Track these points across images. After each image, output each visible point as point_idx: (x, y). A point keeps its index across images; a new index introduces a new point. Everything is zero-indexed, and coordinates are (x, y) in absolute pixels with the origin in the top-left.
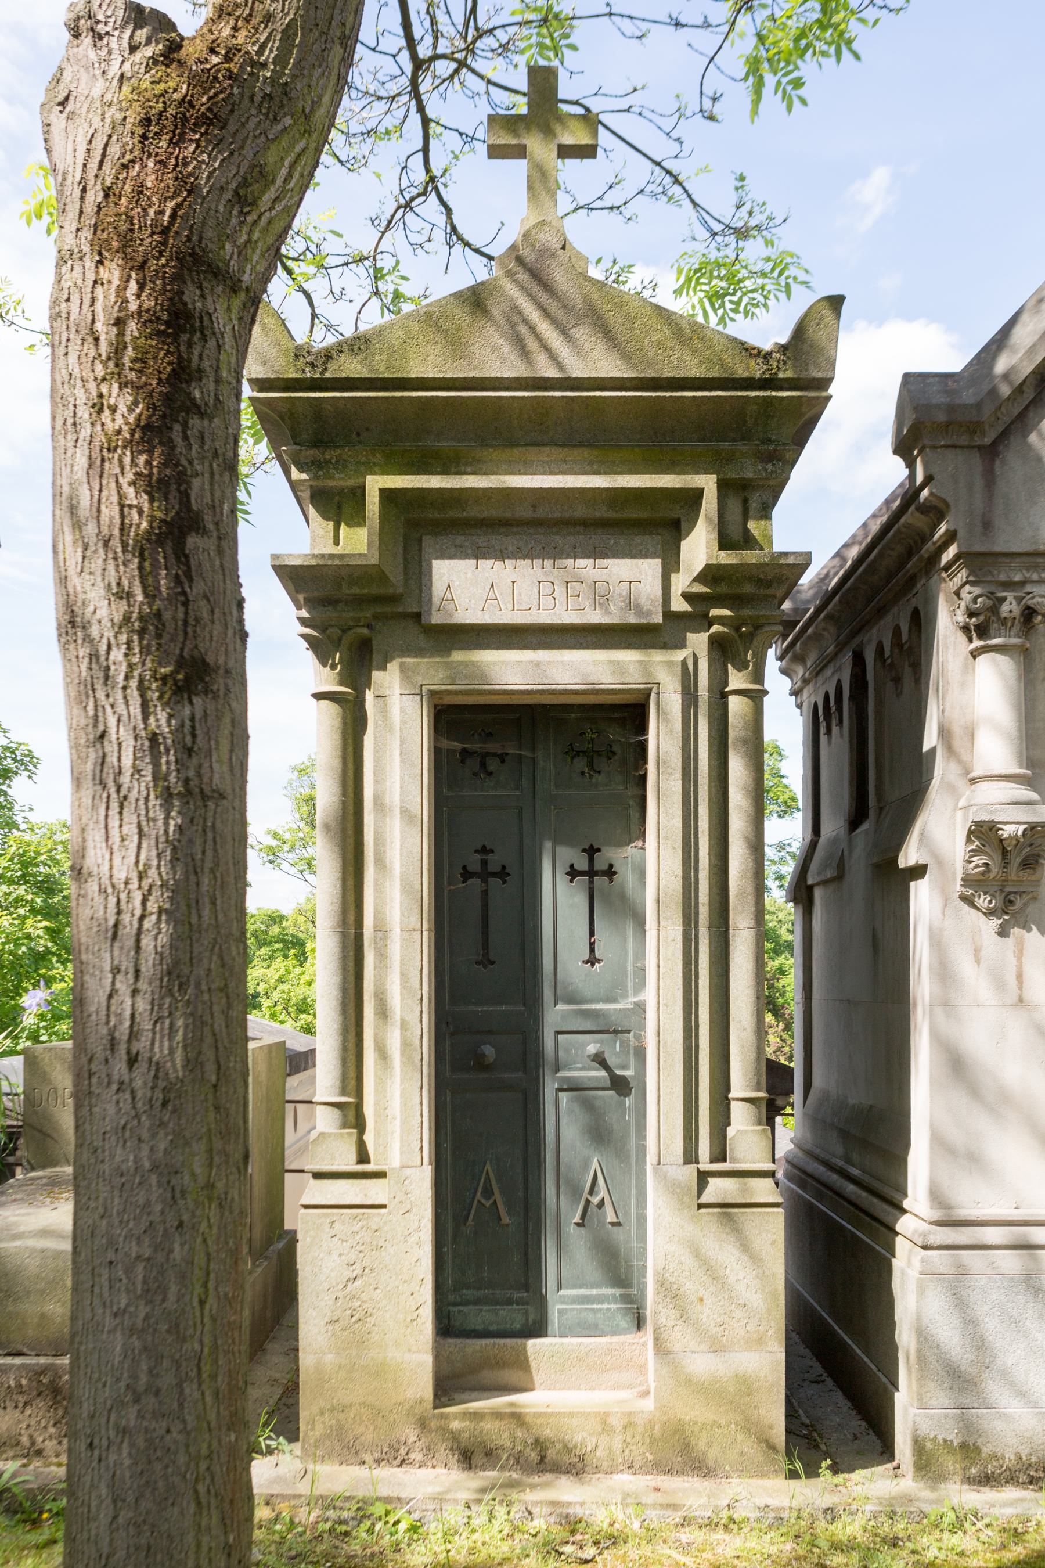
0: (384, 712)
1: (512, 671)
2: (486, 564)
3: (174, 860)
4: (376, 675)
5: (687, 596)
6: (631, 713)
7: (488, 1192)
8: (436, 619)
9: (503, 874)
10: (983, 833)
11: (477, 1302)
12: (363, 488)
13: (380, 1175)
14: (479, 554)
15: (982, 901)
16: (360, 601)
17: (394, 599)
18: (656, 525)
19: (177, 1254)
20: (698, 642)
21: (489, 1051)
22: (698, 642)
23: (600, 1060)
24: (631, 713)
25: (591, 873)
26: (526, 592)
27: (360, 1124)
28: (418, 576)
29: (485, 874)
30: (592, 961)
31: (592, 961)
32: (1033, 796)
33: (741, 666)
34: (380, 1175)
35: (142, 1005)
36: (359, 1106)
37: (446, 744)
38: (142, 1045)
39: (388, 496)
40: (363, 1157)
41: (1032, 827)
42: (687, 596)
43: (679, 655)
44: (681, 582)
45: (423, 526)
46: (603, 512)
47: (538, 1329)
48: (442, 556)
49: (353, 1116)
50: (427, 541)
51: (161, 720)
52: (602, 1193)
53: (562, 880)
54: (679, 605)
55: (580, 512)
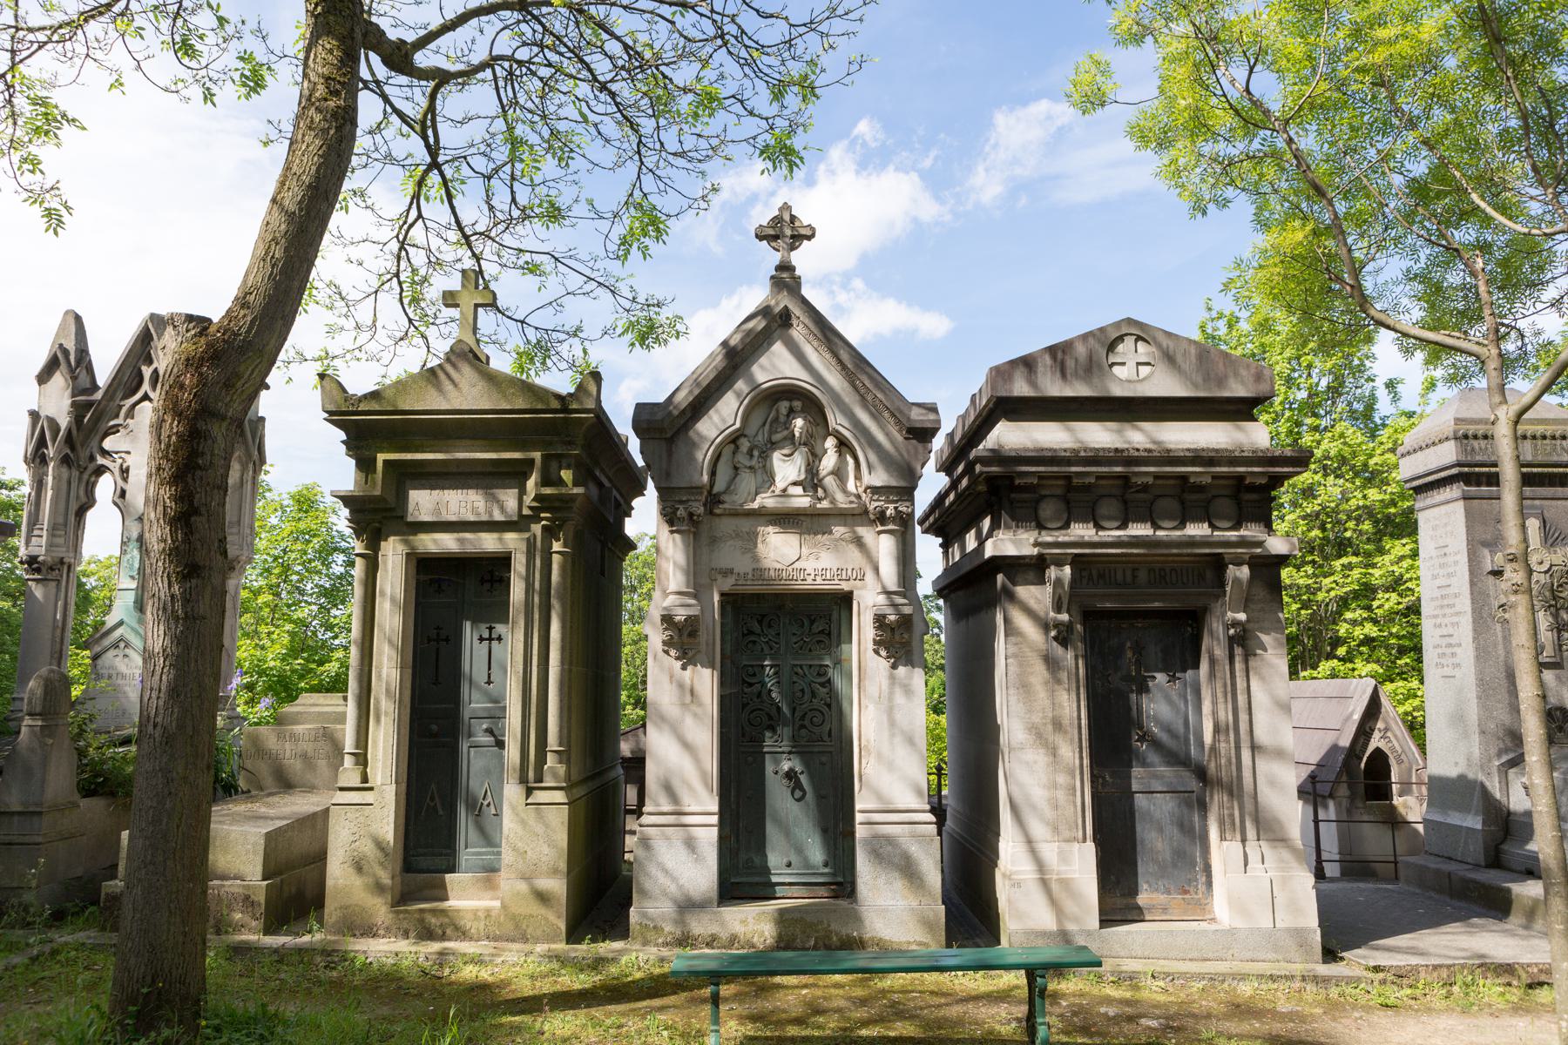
0: (385, 563)
1: (446, 543)
2: (436, 492)
3: (178, 644)
4: (383, 544)
5: (531, 508)
6: (502, 562)
7: (432, 799)
8: (410, 519)
9: (447, 640)
10: (667, 619)
11: (424, 855)
12: (375, 459)
13: (371, 789)
14: (432, 488)
15: (673, 652)
16: (375, 511)
17: (391, 510)
18: (514, 474)
19: (167, 806)
20: (537, 529)
21: (434, 727)
22: (537, 529)
23: (490, 731)
24: (502, 562)
25: (490, 639)
26: (453, 507)
27: (365, 764)
28: (403, 499)
29: (438, 640)
30: (489, 682)
31: (489, 682)
32: (693, 602)
33: (558, 540)
34: (371, 789)
35: (161, 703)
36: (366, 755)
37: (422, 577)
38: (159, 719)
39: (386, 462)
40: (365, 779)
41: (689, 617)
42: (531, 508)
43: (526, 535)
44: (528, 500)
45: (407, 476)
46: (490, 469)
47: (452, 869)
48: (415, 488)
49: (362, 759)
50: (408, 482)
51: (176, 588)
52: (489, 799)
53: (476, 642)
54: (526, 512)
55: (479, 469)
